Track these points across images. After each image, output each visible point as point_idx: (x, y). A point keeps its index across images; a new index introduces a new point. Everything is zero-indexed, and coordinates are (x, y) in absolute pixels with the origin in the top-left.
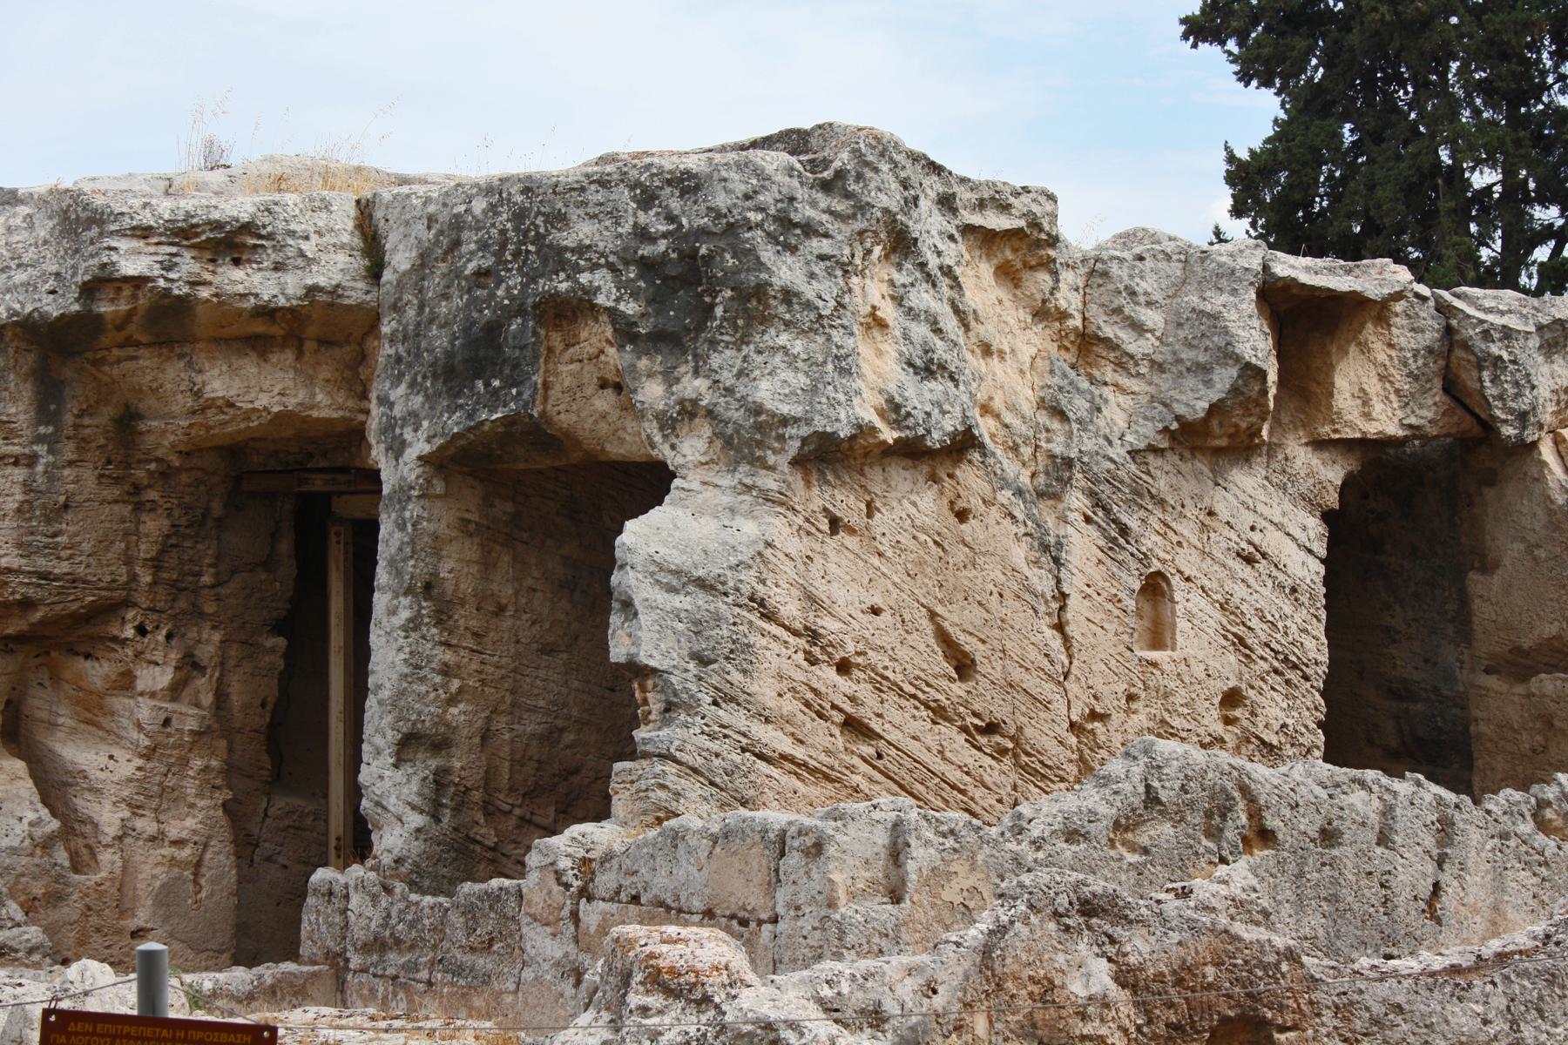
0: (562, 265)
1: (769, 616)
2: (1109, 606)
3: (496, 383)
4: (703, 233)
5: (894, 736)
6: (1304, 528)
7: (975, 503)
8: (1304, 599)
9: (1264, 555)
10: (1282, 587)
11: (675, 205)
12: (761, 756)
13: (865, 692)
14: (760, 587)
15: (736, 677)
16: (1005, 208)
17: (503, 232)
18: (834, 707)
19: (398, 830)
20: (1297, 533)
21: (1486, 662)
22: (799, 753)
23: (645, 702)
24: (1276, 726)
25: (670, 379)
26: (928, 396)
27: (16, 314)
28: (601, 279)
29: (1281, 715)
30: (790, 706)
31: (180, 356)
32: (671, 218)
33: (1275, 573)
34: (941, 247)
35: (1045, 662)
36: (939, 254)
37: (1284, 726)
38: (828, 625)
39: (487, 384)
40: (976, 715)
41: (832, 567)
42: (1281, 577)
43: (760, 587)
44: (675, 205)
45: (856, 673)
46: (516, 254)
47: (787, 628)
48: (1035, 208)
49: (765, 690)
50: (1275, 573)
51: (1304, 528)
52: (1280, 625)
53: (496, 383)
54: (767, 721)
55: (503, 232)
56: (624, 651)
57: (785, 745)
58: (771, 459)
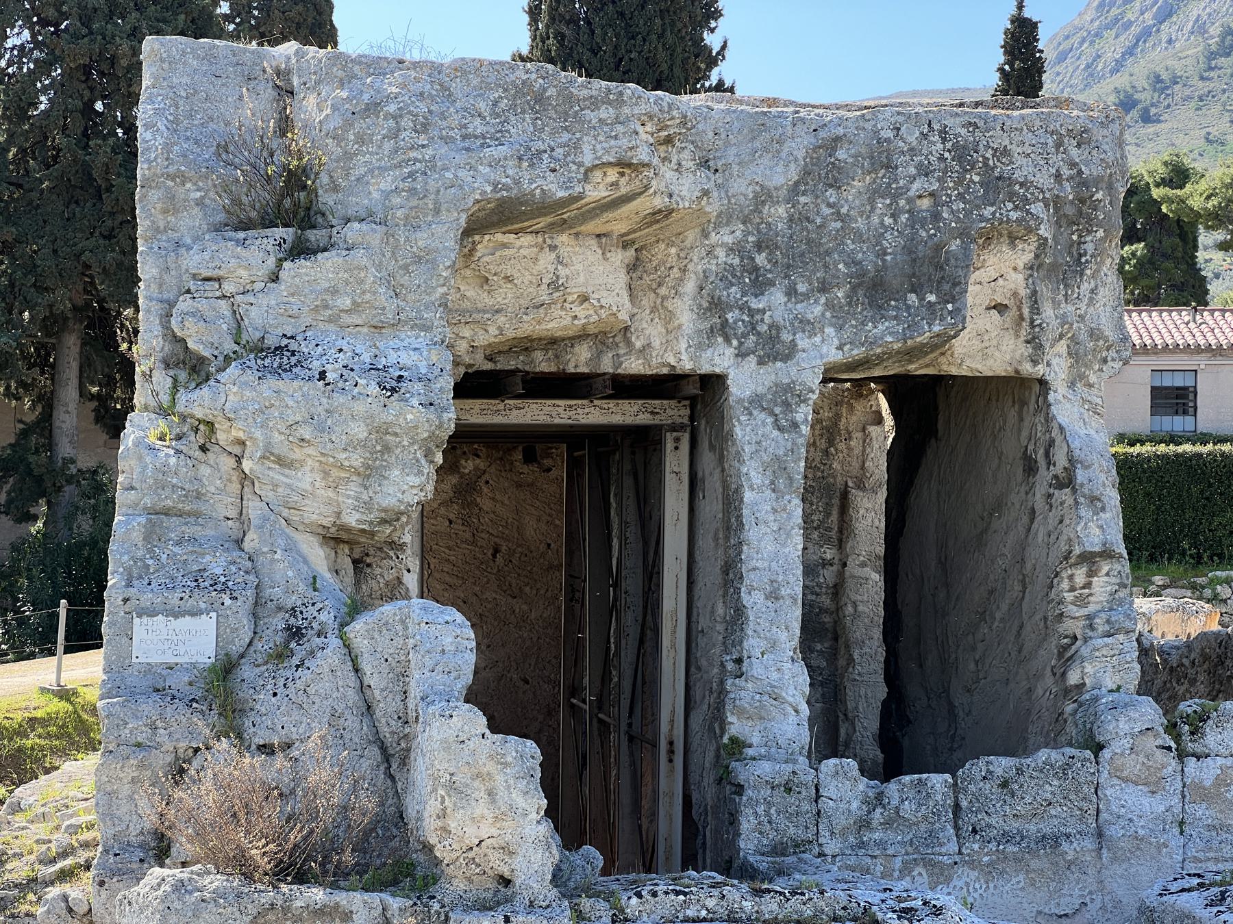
0: (1011, 196)
3: (932, 298)
4: (1097, 181)
11: (1074, 152)
17: (942, 159)
19: (792, 718)
21: (862, 558)
23: (1088, 585)
25: (1056, 304)
27: (506, 187)
28: (1037, 208)
31: (553, 248)
32: (1073, 165)
39: (922, 299)
44: (1074, 152)
46: (960, 182)
53: (932, 298)
55: (942, 159)
56: (1096, 540)
58: (1093, 379)
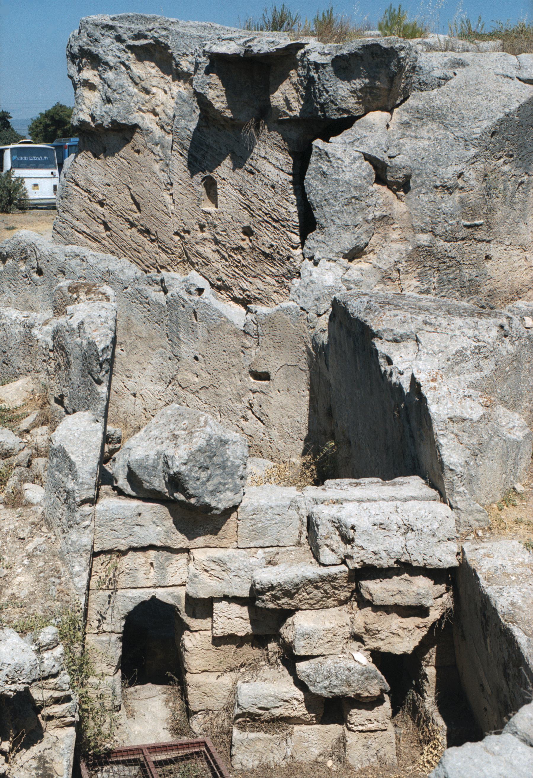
1: (77, 185)
2: (189, 188)
5: (115, 229)
6: (277, 159)
7: (141, 148)
8: (279, 190)
9: (259, 171)
10: (266, 184)
12: (76, 230)
13: (106, 213)
14: (73, 175)
15: (69, 204)
16: (145, 37)
18: (98, 218)
20: (274, 162)
22: (88, 231)
24: (267, 245)
26: (103, 109)
29: (269, 240)
30: (84, 215)
33: (263, 178)
34: (119, 55)
35: (165, 208)
36: (119, 57)
37: (272, 246)
38: (93, 189)
40: (142, 226)
41: (93, 170)
42: (266, 181)
43: (73, 175)
45: (105, 207)
47: (82, 189)
48: (156, 35)
49: (76, 209)
50: (263, 178)
51: (277, 159)
52: (266, 201)
54: (78, 220)
57: (85, 229)
